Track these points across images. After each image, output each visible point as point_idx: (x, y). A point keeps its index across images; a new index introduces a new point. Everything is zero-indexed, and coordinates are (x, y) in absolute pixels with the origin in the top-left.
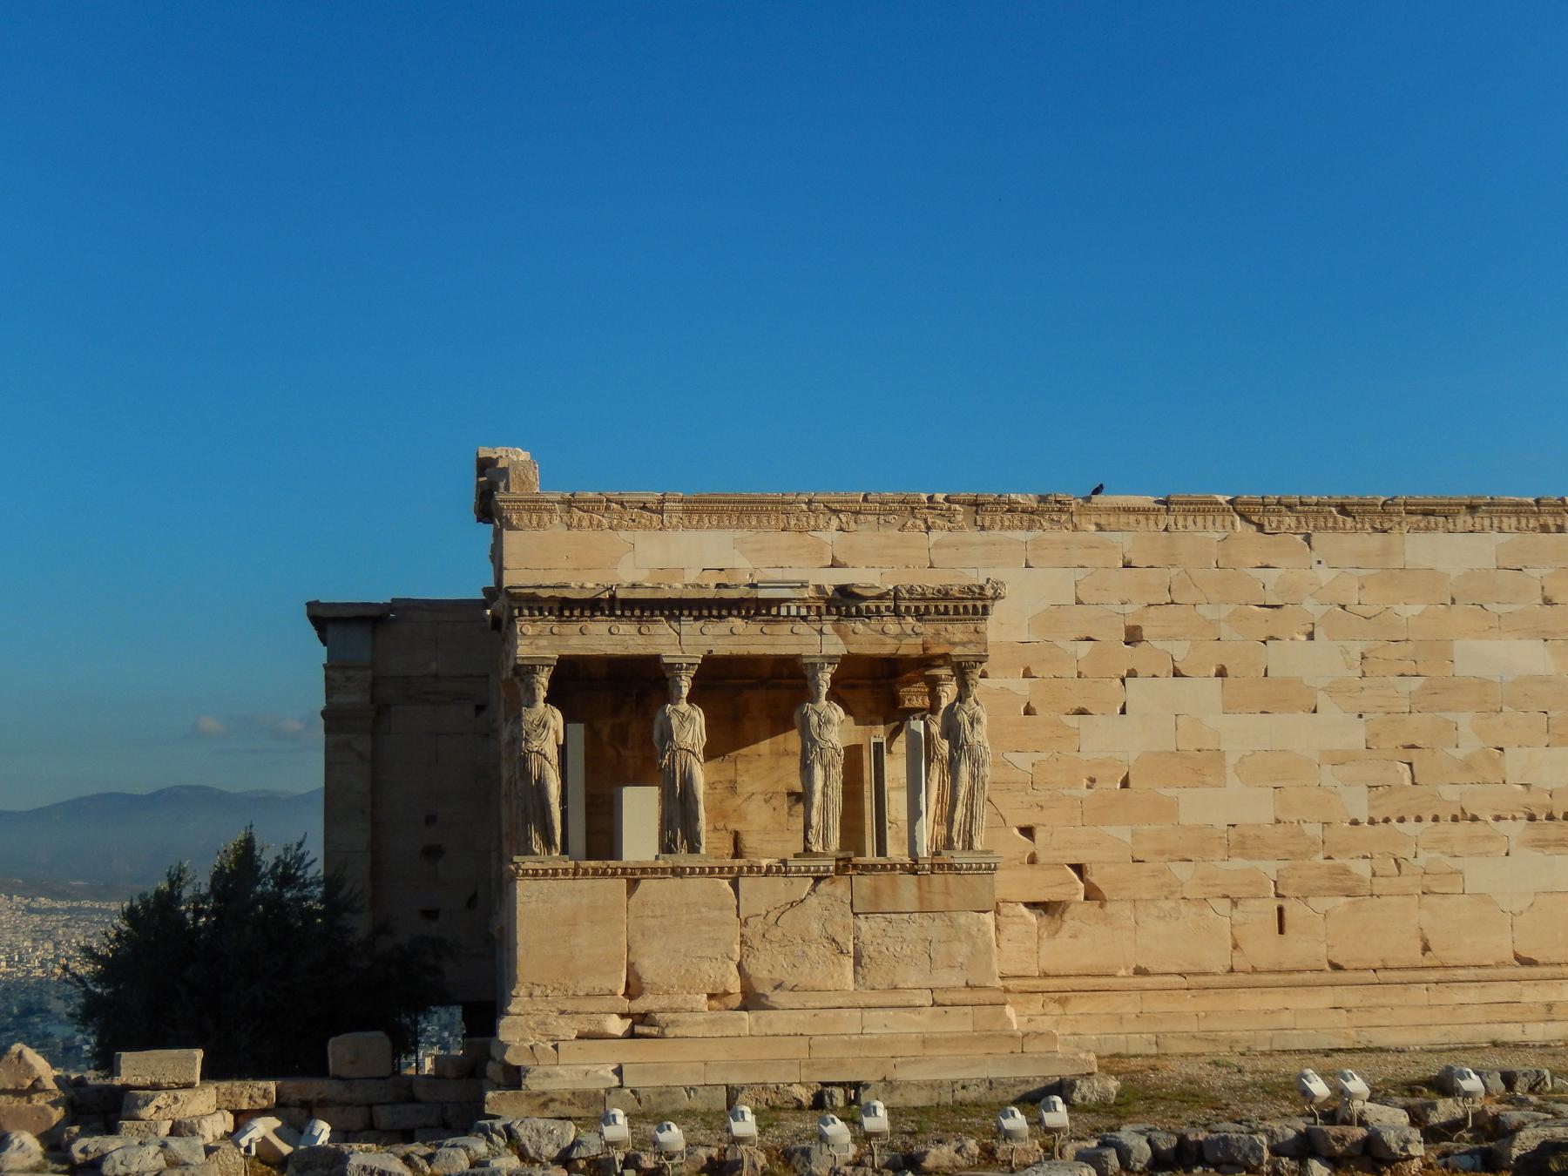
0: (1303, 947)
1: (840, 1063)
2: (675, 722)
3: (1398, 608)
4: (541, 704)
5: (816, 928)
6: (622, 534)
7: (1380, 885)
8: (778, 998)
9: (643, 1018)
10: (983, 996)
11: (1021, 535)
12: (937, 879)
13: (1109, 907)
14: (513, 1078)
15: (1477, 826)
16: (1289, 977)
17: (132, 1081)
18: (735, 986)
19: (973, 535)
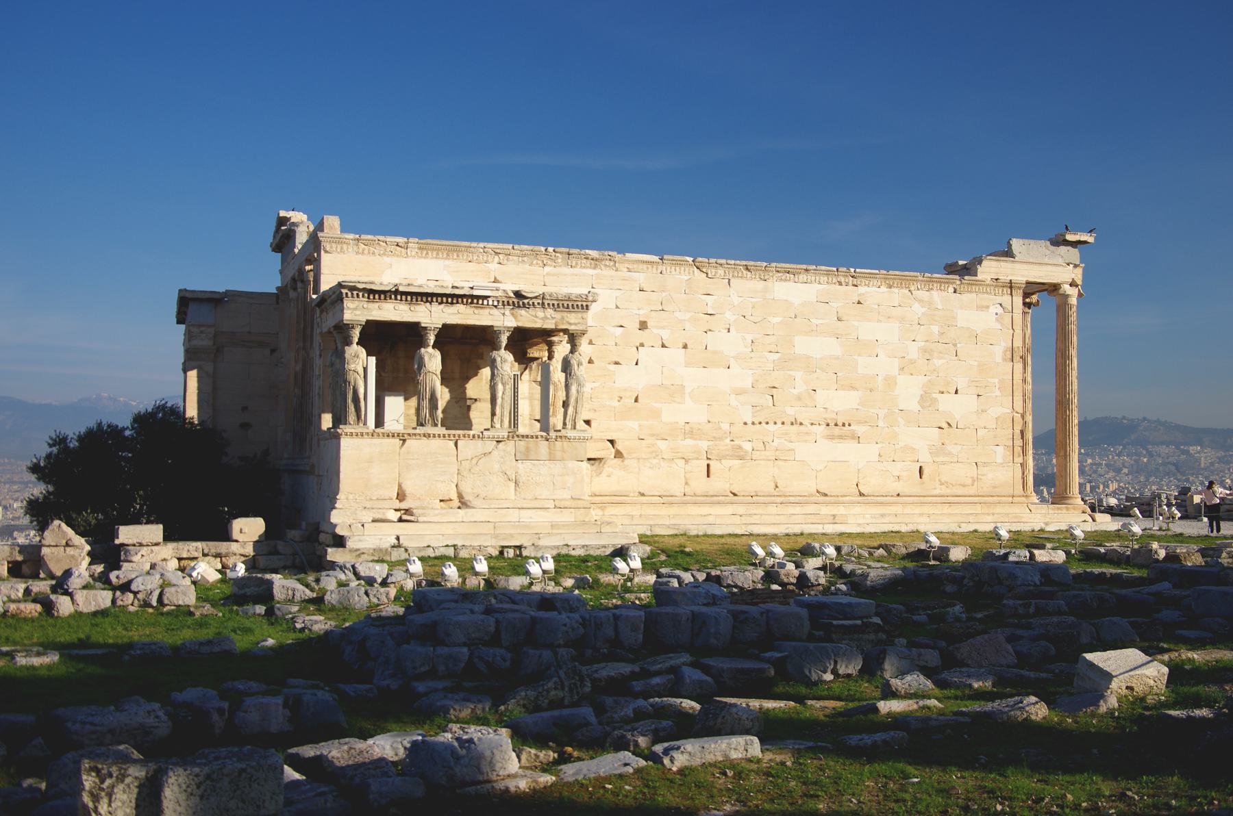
0: (718, 484)
1: (512, 536)
2: (426, 359)
3: (770, 319)
4: (355, 345)
5: (497, 467)
6: (385, 258)
7: (756, 455)
8: (475, 502)
9: (407, 511)
10: (580, 504)
11: (590, 271)
12: (558, 444)
13: (626, 462)
14: (340, 542)
15: (802, 428)
16: (711, 499)
17: (126, 542)
18: (454, 496)
19: (567, 270)
